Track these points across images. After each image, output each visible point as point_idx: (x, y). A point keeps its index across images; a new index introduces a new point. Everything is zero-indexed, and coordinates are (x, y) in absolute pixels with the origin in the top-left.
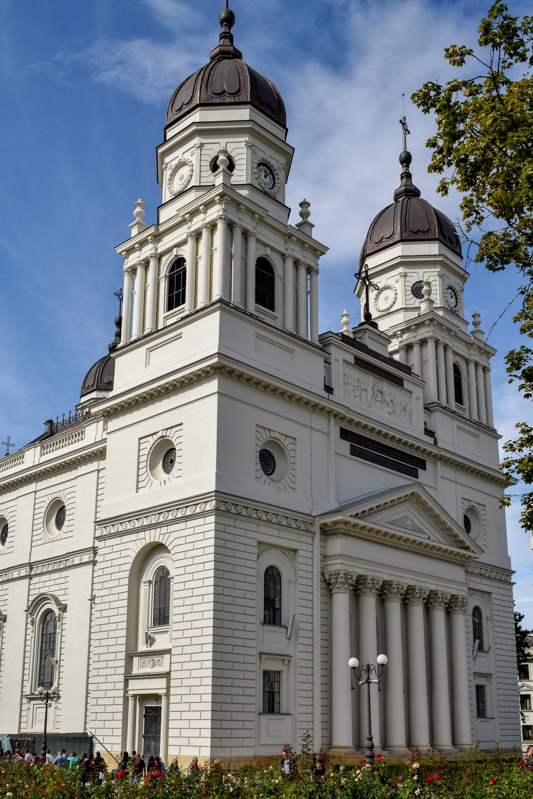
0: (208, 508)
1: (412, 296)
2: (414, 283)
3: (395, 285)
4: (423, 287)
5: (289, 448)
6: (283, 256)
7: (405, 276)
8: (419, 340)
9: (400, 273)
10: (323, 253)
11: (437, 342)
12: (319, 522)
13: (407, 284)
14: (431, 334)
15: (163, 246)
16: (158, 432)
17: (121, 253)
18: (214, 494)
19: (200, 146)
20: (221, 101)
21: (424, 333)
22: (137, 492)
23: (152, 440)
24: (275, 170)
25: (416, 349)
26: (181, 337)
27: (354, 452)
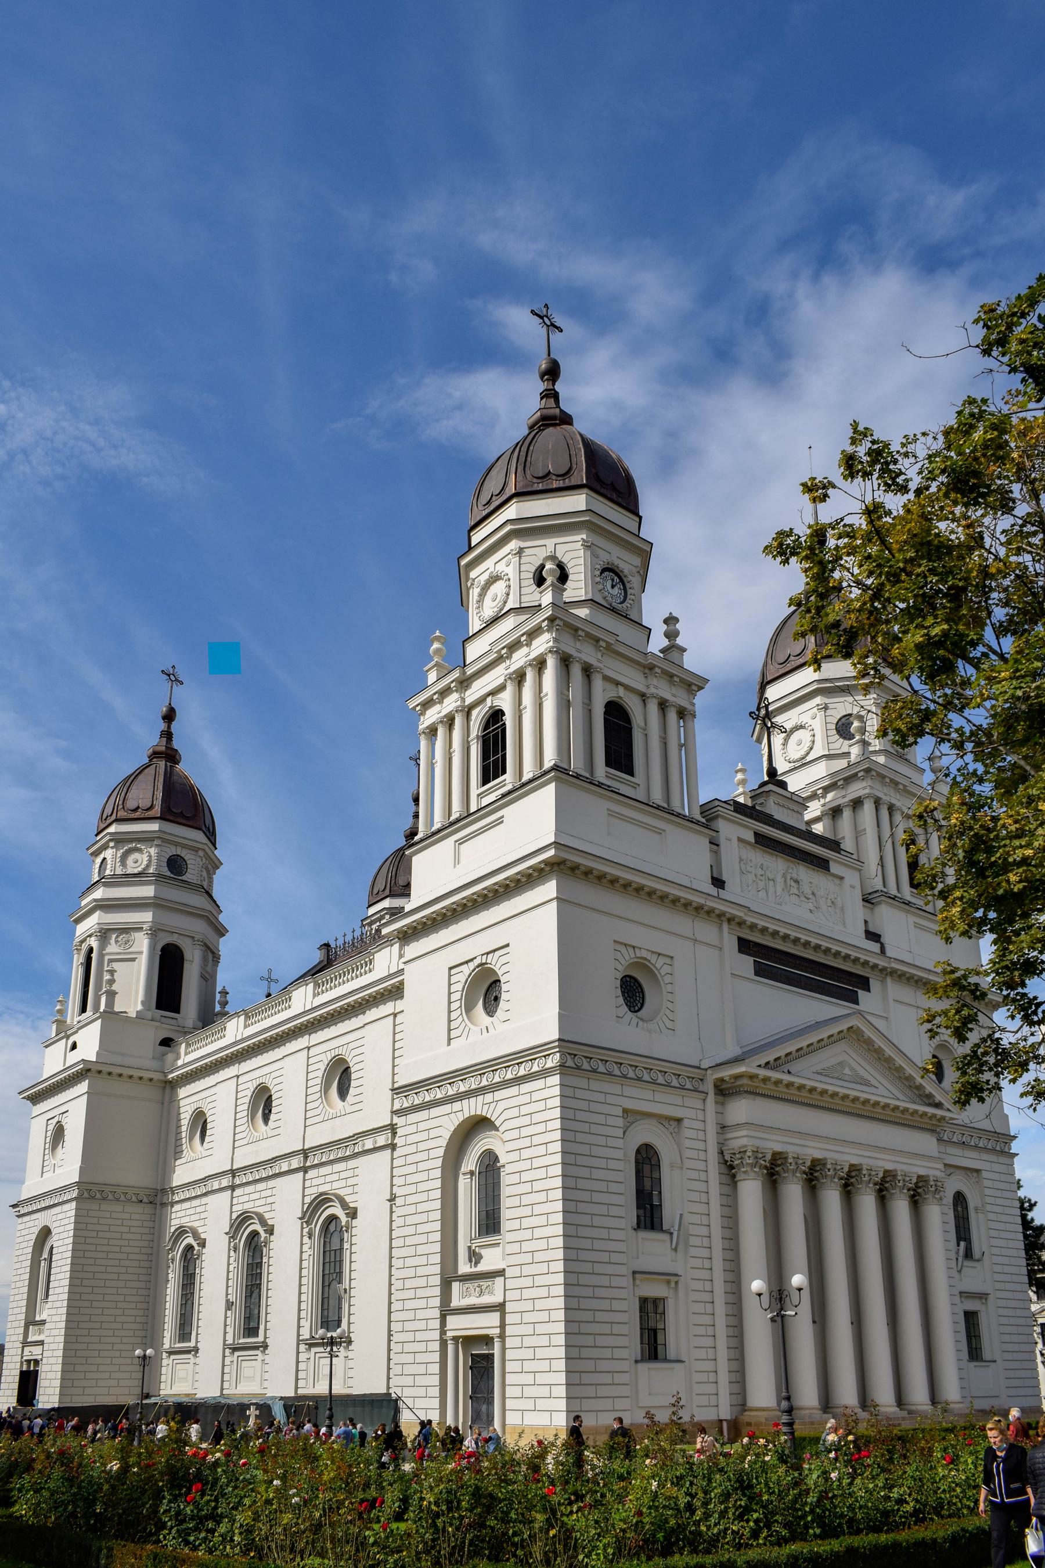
0: (550, 1064)
1: (837, 737)
2: (839, 717)
3: (811, 722)
4: (852, 723)
5: (663, 972)
6: (643, 697)
7: (826, 708)
8: (851, 801)
9: (818, 705)
10: (700, 688)
11: (877, 802)
12: (712, 1076)
13: (829, 719)
14: (867, 791)
15: (472, 694)
16: (475, 958)
17: (414, 708)
18: (557, 1044)
19: (518, 552)
20: (545, 488)
21: (857, 789)
22: (449, 1044)
23: (466, 970)
24: (626, 576)
25: (847, 814)
26: (502, 822)
27: (760, 971)
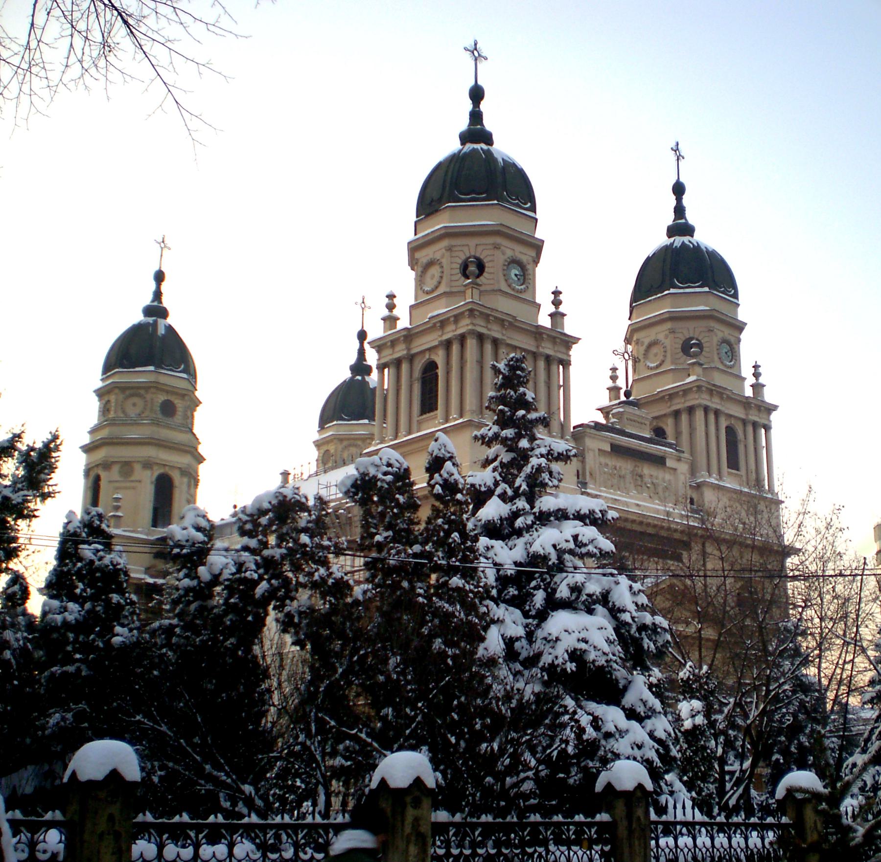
3: (663, 340)
11: (706, 409)
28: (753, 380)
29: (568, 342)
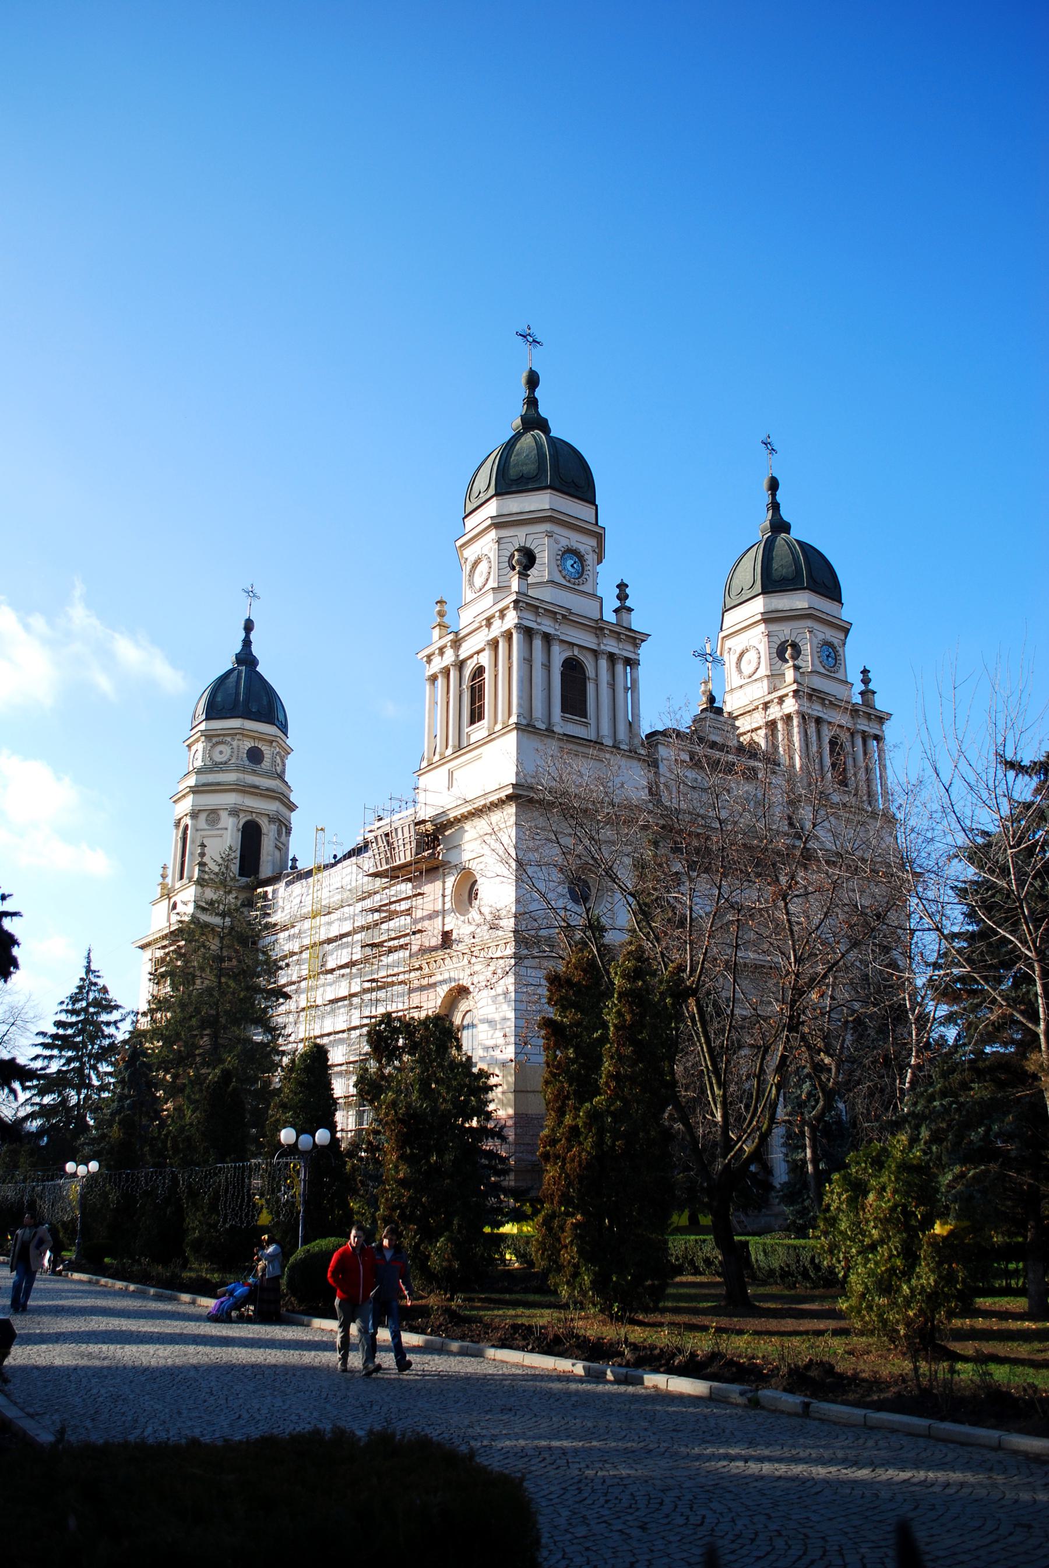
6: (596, 653)
17: (422, 659)
28: (862, 687)
29: (636, 639)
